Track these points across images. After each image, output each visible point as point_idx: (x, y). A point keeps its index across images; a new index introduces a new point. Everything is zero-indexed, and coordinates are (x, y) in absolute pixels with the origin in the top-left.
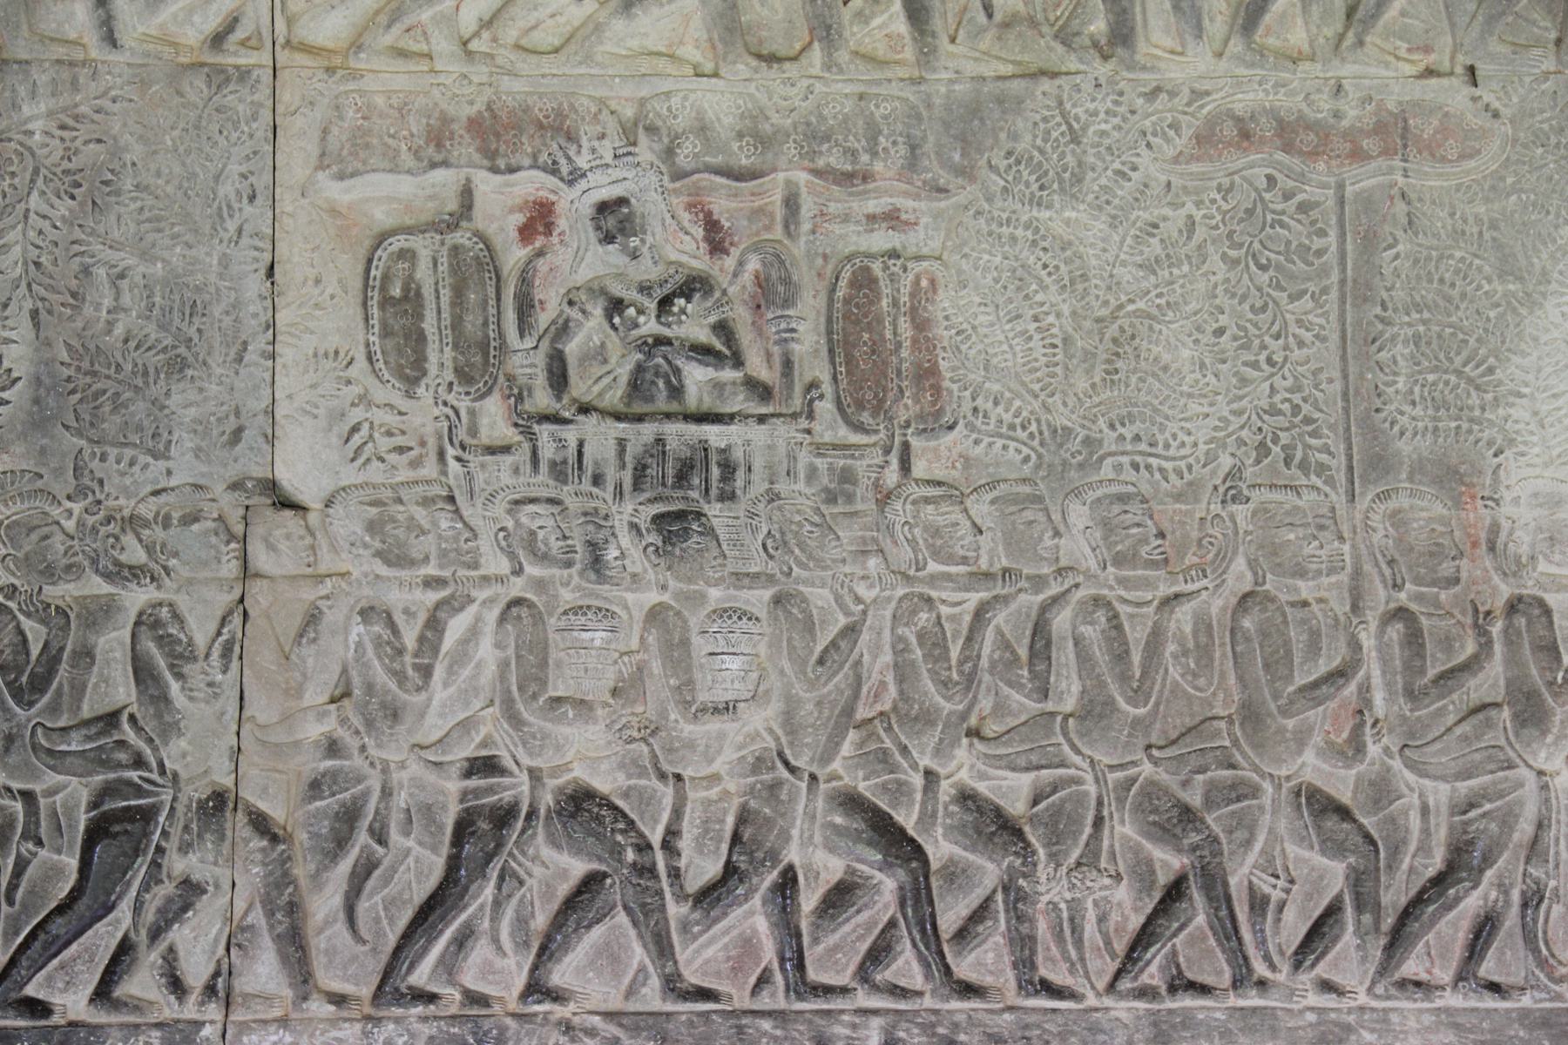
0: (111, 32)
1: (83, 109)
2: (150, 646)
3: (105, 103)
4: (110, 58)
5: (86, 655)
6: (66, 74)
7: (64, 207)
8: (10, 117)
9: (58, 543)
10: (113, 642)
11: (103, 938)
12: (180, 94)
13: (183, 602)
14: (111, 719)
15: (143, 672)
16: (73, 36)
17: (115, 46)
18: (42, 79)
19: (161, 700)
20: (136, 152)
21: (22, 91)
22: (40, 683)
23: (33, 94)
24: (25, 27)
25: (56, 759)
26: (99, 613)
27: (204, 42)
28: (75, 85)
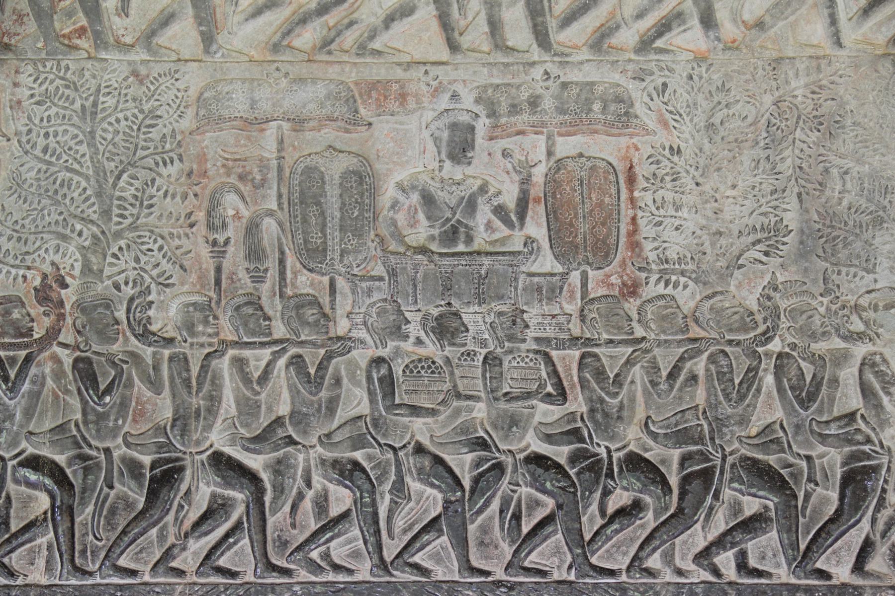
0: (839, 39)
1: (824, 82)
2: (870, 377)
3: (836, 78)
4: (838, 53)
5: (835, 382)
6: (814, 63)
7: (814, 136)
8: (784, 88)
9: (817, 320)
10: (849, 374)
11: (855, 538)
12: (876, 71)
13: (887, 352)
14: (851, 416)
15: (866, 391)
16: (815, 42)
17: (841, 47)
18: (802, 67)
19: (879, 407)
20: (853, 104)
21: (791, 74)
22: (812, 397)
23: (797, 75)
24: (791, 39)
25: (823, 439)
26: (841, 359)
27: (889, 42)
28: (819, 68)
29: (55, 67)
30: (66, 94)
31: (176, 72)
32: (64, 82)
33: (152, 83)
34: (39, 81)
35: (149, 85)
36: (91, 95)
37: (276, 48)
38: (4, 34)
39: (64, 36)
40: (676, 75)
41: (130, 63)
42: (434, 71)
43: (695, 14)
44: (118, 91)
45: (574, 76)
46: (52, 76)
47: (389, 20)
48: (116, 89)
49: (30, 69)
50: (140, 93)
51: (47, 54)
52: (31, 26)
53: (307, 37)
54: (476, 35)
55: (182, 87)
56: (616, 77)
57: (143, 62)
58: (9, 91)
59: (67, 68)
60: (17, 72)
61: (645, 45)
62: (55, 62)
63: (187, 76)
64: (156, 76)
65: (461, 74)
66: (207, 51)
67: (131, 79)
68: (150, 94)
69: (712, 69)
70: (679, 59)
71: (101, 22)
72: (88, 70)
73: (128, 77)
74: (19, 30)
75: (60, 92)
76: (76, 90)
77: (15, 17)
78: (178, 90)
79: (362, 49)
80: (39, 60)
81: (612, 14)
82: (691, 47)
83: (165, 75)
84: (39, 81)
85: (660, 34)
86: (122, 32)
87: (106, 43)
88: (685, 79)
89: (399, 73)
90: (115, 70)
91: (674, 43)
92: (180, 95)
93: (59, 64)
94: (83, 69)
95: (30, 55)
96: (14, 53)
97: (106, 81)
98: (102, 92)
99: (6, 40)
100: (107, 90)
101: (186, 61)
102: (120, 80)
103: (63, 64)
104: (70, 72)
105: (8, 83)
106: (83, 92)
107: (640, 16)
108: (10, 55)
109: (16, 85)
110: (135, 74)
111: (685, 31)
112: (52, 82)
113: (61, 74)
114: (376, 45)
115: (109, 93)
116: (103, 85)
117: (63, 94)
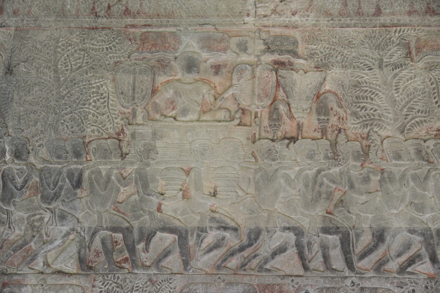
29: (113, 277)
30: (117, 291)
31: (170, 279)
32: (116, 285)
33: (158, 285)
34: (105, 284)
35: (157, 286)
36: (129, 291)
37: (219, 267)
38: (89, 262)
39: (117, 262)
40: (419, 286)
41: (148, 275)
42: (296, 280)
43: (427, 256)
44: (142, 289)
45: (367, 284)
46: (111, 282)
47: (274, 254)
48: (141, 288)
49: (101, 278)
50: (153, 290)
51: (109, 271)
52: (102, 258)
53: (234, 262)
54: (317, 262)
55: (173, 287)
56: (388, 286)
57: (154, 274)
58: (90, 289)
59: (118, 278)
60: (94, 280)
61: (402, 270)
62: (113, 275)
63: (175, 281)
64: (161, 281)
65: (310, 282)
66: (185, 269)
67: (148, 283)
68: (157, 290)
69: (437, 284)
70: (420, 277)
71: (135, 255)
72: (128, 278)
73: (147, 282)
74: (97, 259)
75: (114, 290)
76: (122, 288)
77: (95, 254)
78: (171, 288)
79: (261, 268)
80: (105, 274)
81: (385, 255)
82: (426, 272)
83: (165, 281)
84: (105, 284)
85: (410, 265)
86: (145, 260)
87: (137, 265)
88: (424, 288)
89: (279, 281)
90: (141, 278)
91: (417, 270)
92: (171, 291)
93: (114, 276)
94: (126, 278)
95: (101, 272)
96: (94, 271)
97: (136, 284)
98: (134, 289)
99: (90, 264)
100: (137, 288)
101: (175, 274)
102: (143, 283)
103: (116, 276)
104: (120, 280)
105: (90, 286)
106: (125, 290)
107: (399, 255)
108: (92, 272)
109: (94, 286)
110: (150, 280)
111: (422, 264)
112: (111, 284)
113: (115, 281)
114: (268, 266)
115: (138, 290)
116: (135, 286)
117: (116, 290)
